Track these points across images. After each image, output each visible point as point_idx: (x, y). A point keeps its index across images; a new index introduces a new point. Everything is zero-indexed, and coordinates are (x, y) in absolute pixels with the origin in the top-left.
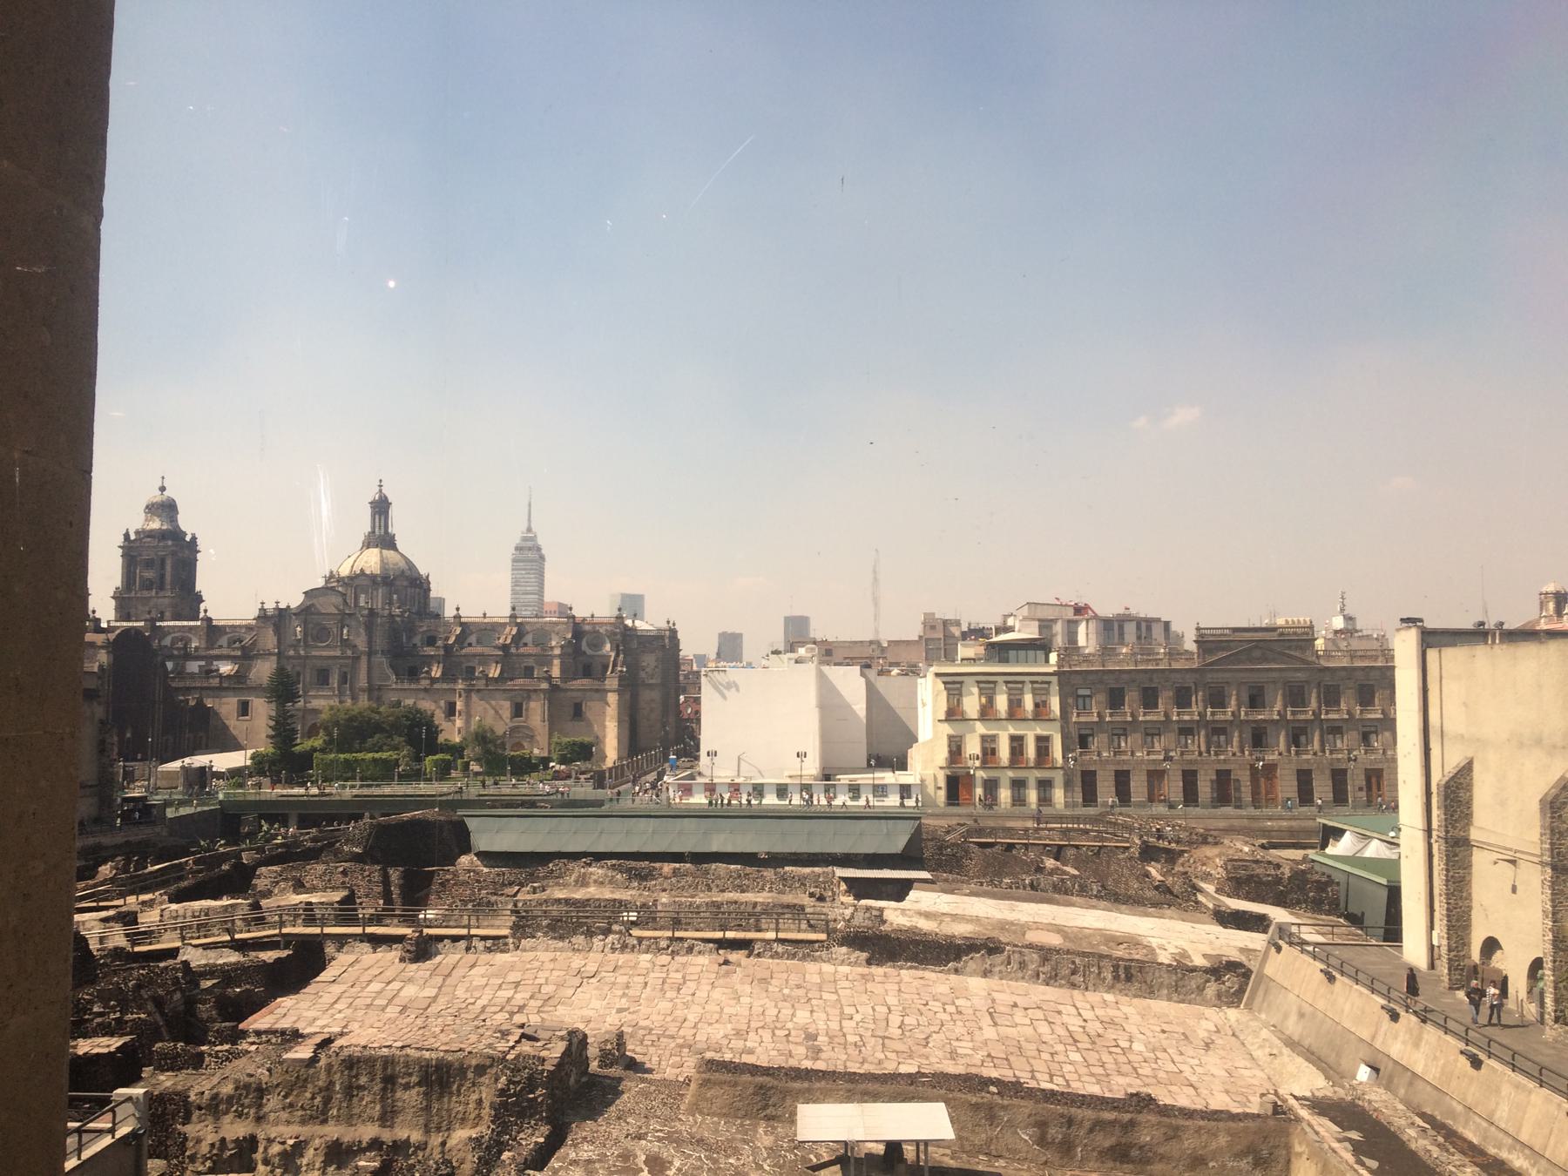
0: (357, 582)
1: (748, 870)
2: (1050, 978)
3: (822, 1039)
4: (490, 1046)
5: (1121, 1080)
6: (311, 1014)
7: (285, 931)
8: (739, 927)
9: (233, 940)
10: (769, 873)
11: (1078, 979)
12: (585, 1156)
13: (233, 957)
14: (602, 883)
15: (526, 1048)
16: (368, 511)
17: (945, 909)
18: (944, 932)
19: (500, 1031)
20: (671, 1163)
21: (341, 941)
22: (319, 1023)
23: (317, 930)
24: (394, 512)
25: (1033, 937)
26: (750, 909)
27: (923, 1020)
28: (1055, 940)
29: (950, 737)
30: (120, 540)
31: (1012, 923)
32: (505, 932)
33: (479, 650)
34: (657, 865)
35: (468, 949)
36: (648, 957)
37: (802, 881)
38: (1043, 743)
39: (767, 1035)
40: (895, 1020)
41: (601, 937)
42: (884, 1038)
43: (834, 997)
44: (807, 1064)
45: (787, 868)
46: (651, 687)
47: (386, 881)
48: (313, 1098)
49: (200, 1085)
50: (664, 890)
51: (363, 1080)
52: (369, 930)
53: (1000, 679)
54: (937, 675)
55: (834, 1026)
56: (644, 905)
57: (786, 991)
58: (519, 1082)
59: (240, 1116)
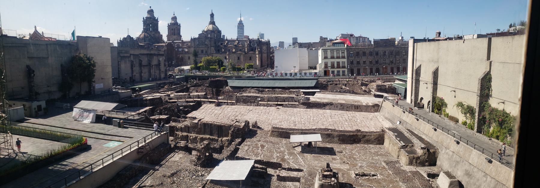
0: (207, 32)
4: (230, 123)
7: (194, 99)
9: (186, 100)
10: (287, 91)
15: (237, 123)
17: (323, 97)
19: (232, 120)
20: (265, 146)
21: (204, 102)
22: (200, 116)
23: (200, 100)
25: (339, 102)
27: (317, 118)
28: (343, 102)
31: (335, 99)
32: (234, 102)
33: (231, 46)
36: (263, 107)
39: (286, 122)
40: (312, 119)
42: (309, 122)
43: (300, 115)
44: (294, 128)
45: (291, 90)
47: (213, 90)
52: (209, 100)
53: (335, 50)
55: (300, 120)
57: (290, 114)
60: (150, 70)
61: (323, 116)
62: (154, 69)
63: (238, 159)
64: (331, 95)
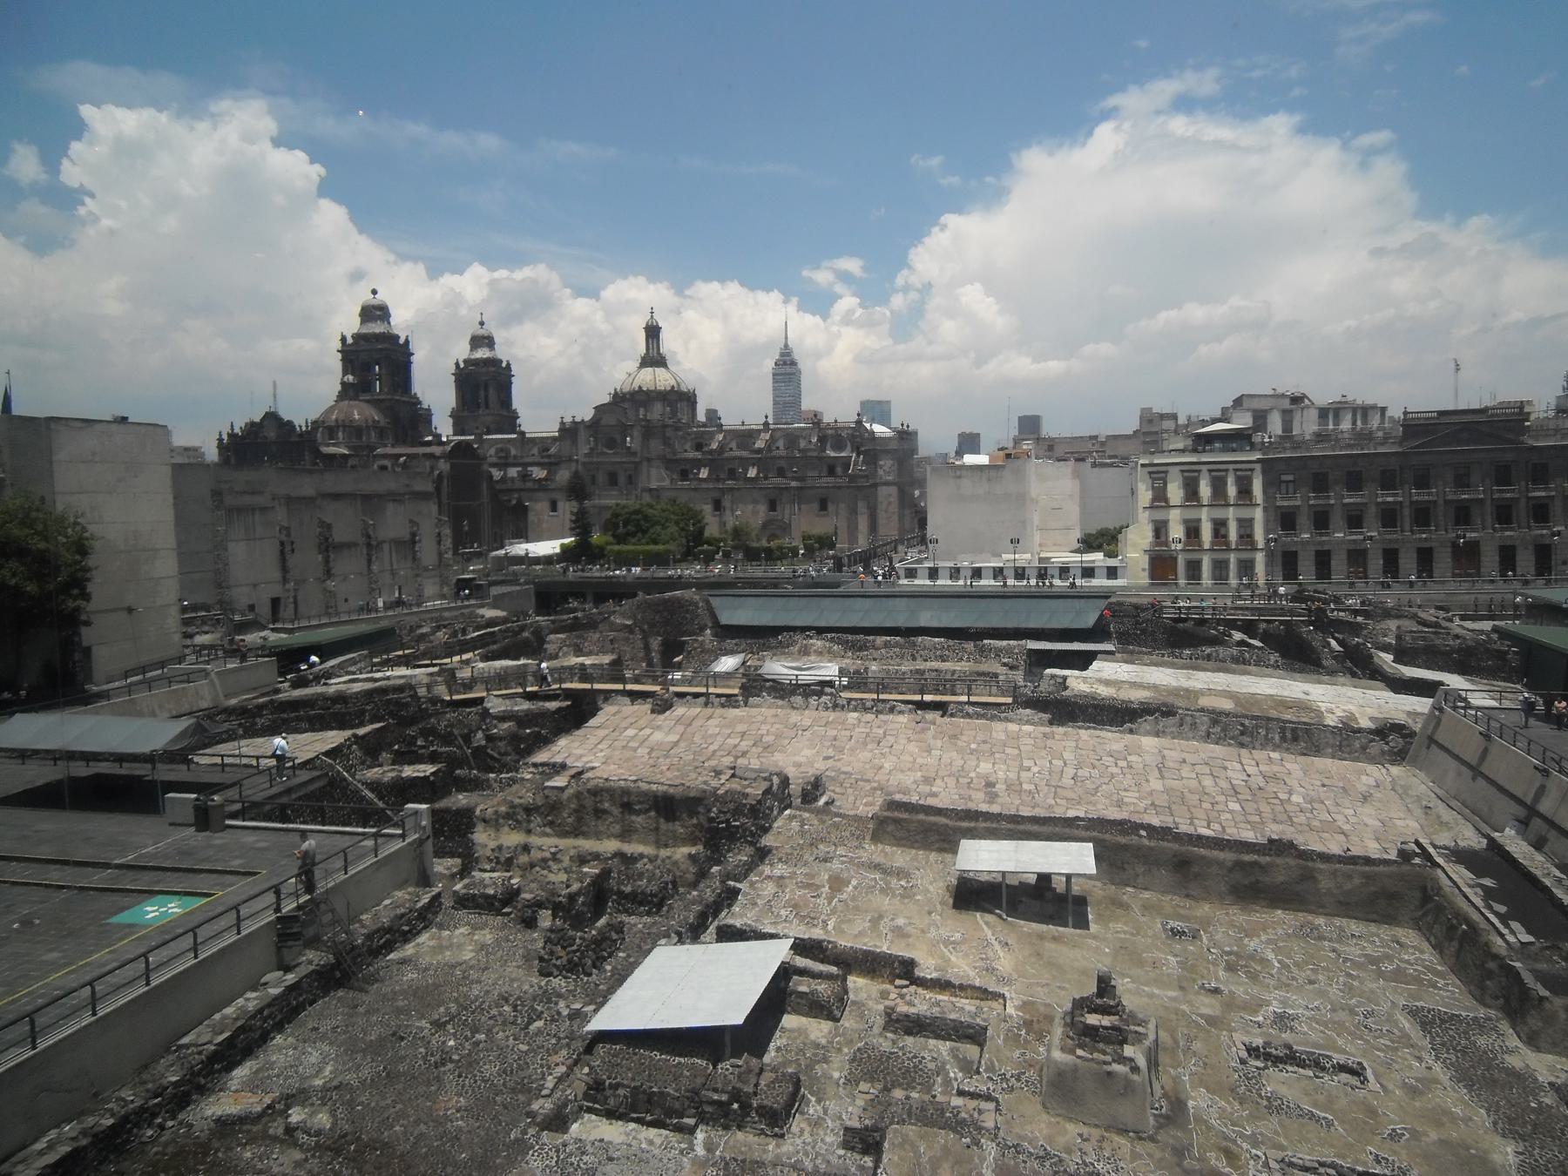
1: (951, 642)
3: (1000, 787)
4: (705, 783)
5: (1275, 827)
6: (579, 752)
7: (564, 686)
8: (937, 692)
10: (970, 646)
11: (1246, 739)
12: (777, 872)
13: (525, 706)
15: (735, 785)
16: (642, 336)
17: (1125, 677)
18: (1121, 697)
20: (849, 883)
21: (608, 695)
22: (585, 759)
23: (588, 686)
24: (664, 336)
25: (1204, 702)
26: (948, 677)
27: (1095, 773)
28: (1227, 705)
30: (453, 369)
32: (736, 691)
34: (871, 638)
36: (855, 715)
37: (998, 652)
38: (1246, 525)
39: (951, 782)
40: (1070, 771)
42: (1056, 787)
43: (1016, 752)
44: (984, 807)
45: (985, 641)
46: (887, 484)
47: (647, 648)
49: (484, 804)
50: (875, 659)
52: (629, 687)
55: (1012, 775)
56: (857, 672)
57: (973, 746)
61: (1122, 764)
63: (729, 934)
64: (1169, 671)
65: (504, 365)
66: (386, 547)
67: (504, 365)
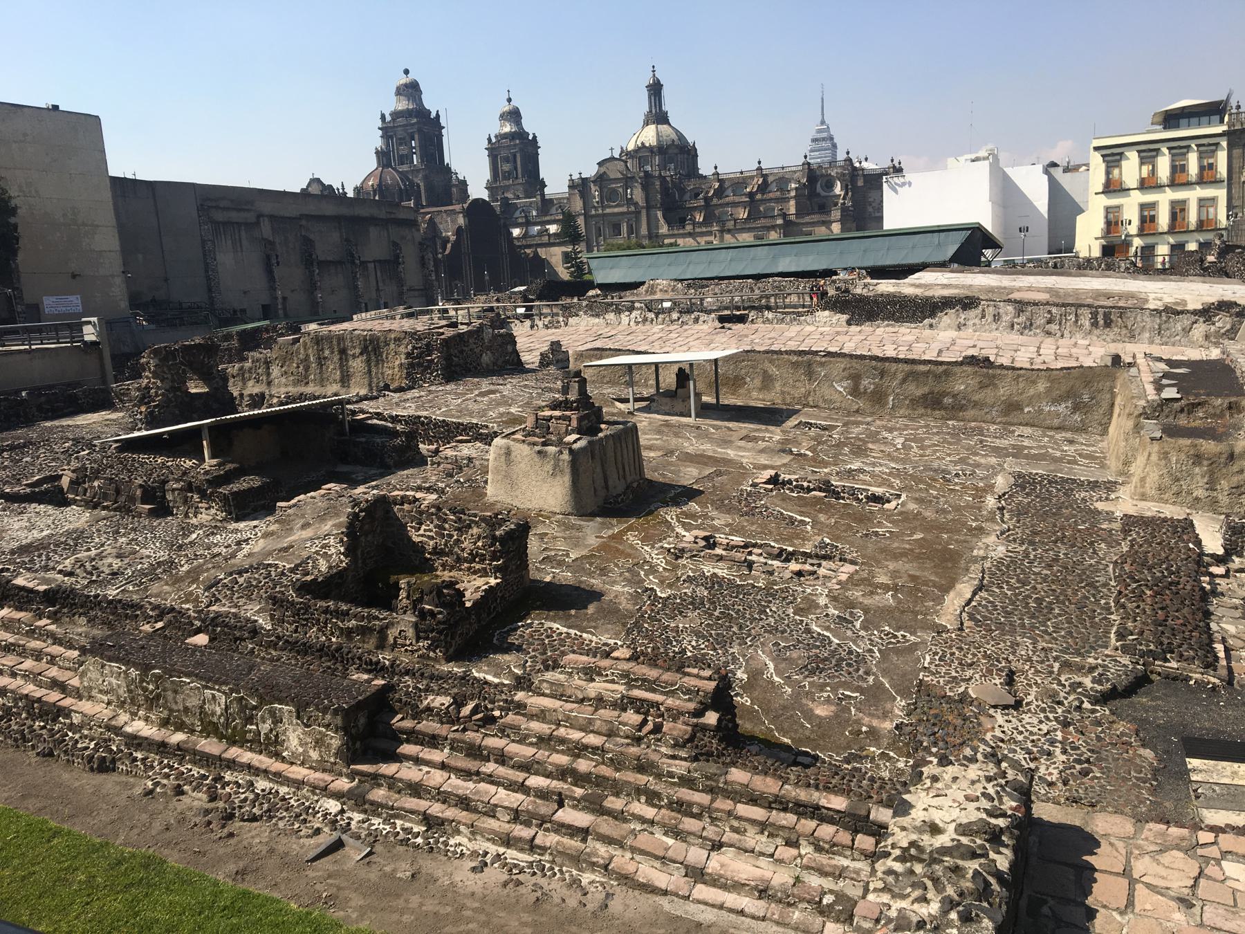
0: (641, 153)
2: (1025, 328)
11: (1054, 327)
14: (666, 291)
16: (646, 94)
24: (666, 92)
29: (1108, 210)
35: (532, 327)
41: (627, 313)
48: (298, 367)
51: (327, 353)
54: (1096, 149)
58: (420, 348)
59: (258, 382)
60: (355, 278)
62: (372, 279)
65: (530, 137)
66: (371, 266)
67: (530, 137)
